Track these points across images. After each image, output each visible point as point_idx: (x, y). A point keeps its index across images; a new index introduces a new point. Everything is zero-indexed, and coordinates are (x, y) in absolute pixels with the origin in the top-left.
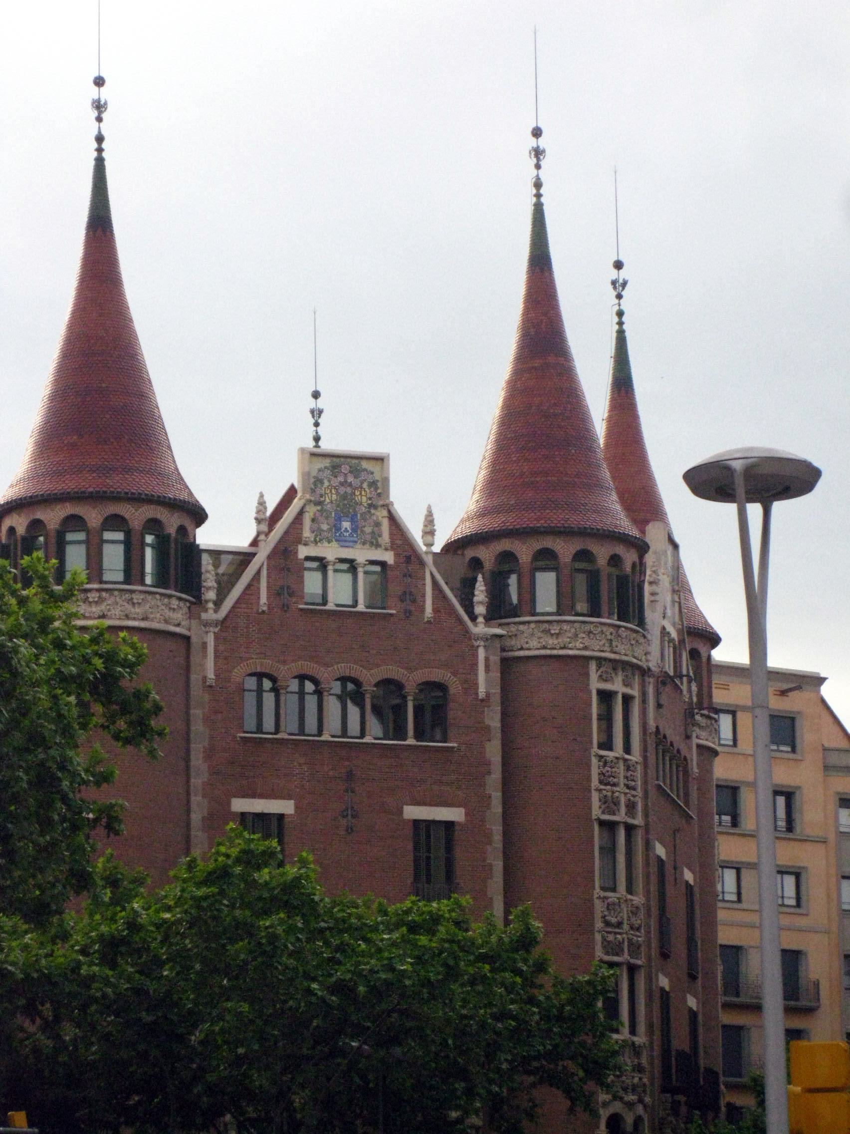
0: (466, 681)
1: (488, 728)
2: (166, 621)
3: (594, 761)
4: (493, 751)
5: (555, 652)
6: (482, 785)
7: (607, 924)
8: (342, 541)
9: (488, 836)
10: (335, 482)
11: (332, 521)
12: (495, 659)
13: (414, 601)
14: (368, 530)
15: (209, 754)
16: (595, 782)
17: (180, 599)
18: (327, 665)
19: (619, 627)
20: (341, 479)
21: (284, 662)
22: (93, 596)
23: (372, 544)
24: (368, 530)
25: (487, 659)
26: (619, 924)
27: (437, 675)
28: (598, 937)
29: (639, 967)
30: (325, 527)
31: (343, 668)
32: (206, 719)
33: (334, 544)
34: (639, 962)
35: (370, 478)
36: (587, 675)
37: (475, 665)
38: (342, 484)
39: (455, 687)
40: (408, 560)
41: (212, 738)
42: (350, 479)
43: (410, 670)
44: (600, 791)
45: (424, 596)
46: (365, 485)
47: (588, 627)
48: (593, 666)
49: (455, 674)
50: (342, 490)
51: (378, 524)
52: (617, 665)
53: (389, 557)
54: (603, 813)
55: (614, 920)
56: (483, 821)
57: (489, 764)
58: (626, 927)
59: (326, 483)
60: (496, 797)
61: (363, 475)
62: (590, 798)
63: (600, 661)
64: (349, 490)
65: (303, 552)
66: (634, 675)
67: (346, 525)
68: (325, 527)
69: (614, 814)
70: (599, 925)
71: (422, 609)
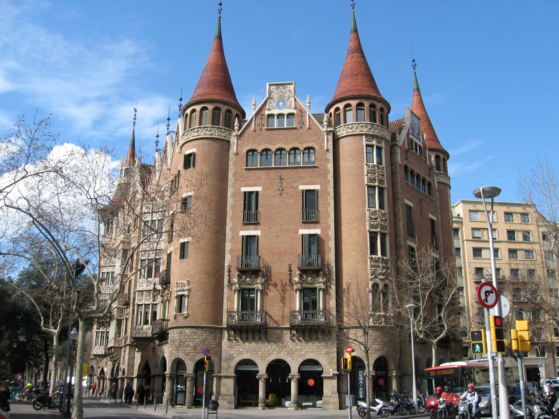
0: (321, 146)
1: (329, 159)
2: (219, 135)
3: (365, 166)
4: (330, 166)
5: (350, 134)
6: (327, 177)
7: (371, 219)
8: (279, 108)
9: (329, 194)
10: (278, 92)
11: (276, 103)
12: (331, 138)
13: (303, 123)
14: (288, 104)
15: (234, 174)
16: (365, 173)
17: (225, 129)
18: (274, 145)
19: (374, 124)
20: (280, 90)
21: (259, 145)
22: (196, 130)
23: (289, 108)
24: (288, 104)
25: (327, 139)
26: (376, 219)
27: (310, 145)
28: (368, 223)
29: (387, 234)
30: (274, 105)
31: (279, 146)
32: (234, 164)
33: (277, 109)
34: (386, 232)
35: (289, 89)
36: (362, 139)
37: (323, 140)
38: (280, 92)
39: (317, 147)
40: (301, 110)
41: (235, 170)
42: (283, 90)
43: (302, 144)
44: (368, 176)
45: (306, 121)
46: (287, 92)
47: (361, 125)
48: (364, 137)
49: (317, 144)
50: (280, 94)
51: (291, 102)
52: (373, 136)
53: (295, 112)
54: (369, 182)
55: (373, 217)
56: (327, 188)
57: (329, 170)
58: (379, 220)
59: (275, 92)
60: (332, 180)
61: (287, 89)
62: (364, 178)
63: (366, 135)
64: (282, 93)
65: (267, 113)
66: (382, 141)
67: (281, 103)
68: (274, 105)
69: (374, 183)
70: (368, 218)
71: (306, 126)
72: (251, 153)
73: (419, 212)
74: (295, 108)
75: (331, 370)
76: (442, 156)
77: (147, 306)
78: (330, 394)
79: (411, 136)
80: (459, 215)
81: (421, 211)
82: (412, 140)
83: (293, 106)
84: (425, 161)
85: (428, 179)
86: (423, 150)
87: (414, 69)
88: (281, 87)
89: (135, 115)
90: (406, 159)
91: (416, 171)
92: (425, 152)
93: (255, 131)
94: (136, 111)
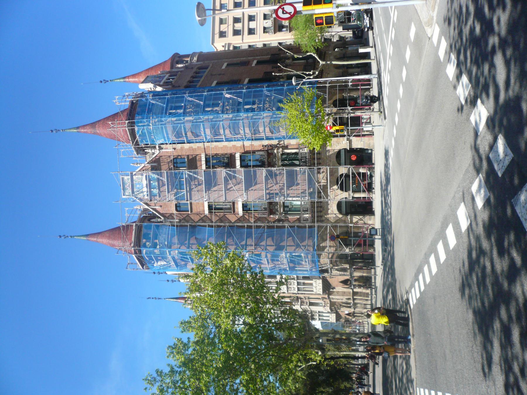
6: (195, 149)
20: (128, 187)
25: (165, 149)
57: (190, 147)
72: (178, 209)
73: (221, 76)
74: (142, 175)
75: (344, 142)
76: (177, 59)
77: (298, 284)
78: (362, 143)
79: (161, 83)
80: (223, 46)
81: (220, 75)
82: (164, 83)
83: (140, 176)
84: (181, 72)
85: (195, 70)
86: (172, 74)
87: (107, 81)
88: (126, 186)
89: (153, 298)
90: (179, 86)
91: (188, 78)
92: (174, 72)
93: (161, 206)
94: (150, 298)
